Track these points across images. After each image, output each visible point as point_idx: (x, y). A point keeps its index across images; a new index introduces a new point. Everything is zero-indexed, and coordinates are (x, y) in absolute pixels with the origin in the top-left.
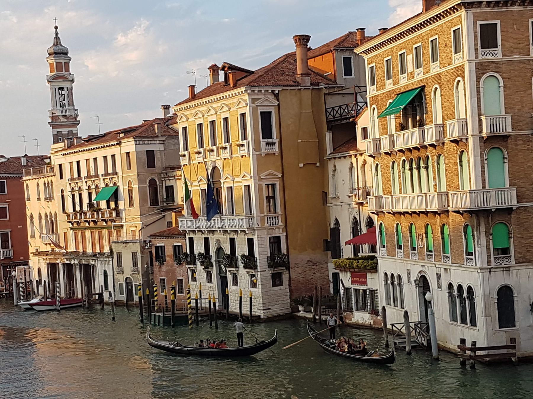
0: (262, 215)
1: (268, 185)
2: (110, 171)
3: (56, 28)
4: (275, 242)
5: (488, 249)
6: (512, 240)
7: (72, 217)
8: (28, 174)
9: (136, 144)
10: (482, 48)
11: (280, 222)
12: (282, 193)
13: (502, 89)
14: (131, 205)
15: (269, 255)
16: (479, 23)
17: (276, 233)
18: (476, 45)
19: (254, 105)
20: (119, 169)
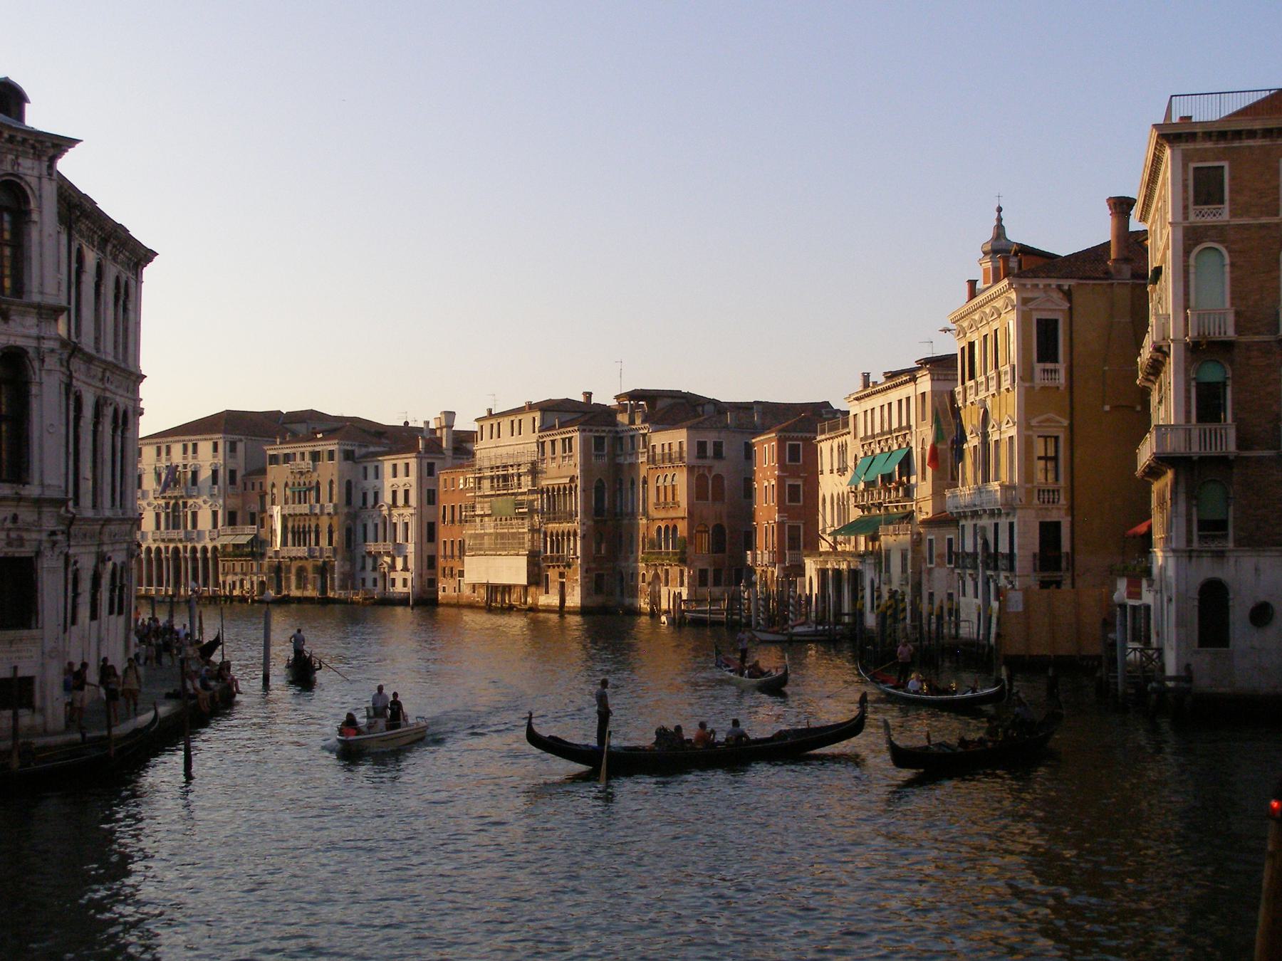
0: (1029, 486)
1: (1046, 437)
2: (904, 424)
3: (1000, 210)
4: (1049, 532)
5: (1189, 522)
6: (1231, 510)
7: (859, 498)
8: (823, 432)
9: (932, 380)
10: (1196, 203)
11: (1062, 498)
12: (1068, 453)
13: (1227, 269)
14: (924, 478)
15: (1037, 550)
16: (1192, 165)
17: (1053, 516)
18: (1185, 199)
19: (1025, 308)
20: (913, 422)
